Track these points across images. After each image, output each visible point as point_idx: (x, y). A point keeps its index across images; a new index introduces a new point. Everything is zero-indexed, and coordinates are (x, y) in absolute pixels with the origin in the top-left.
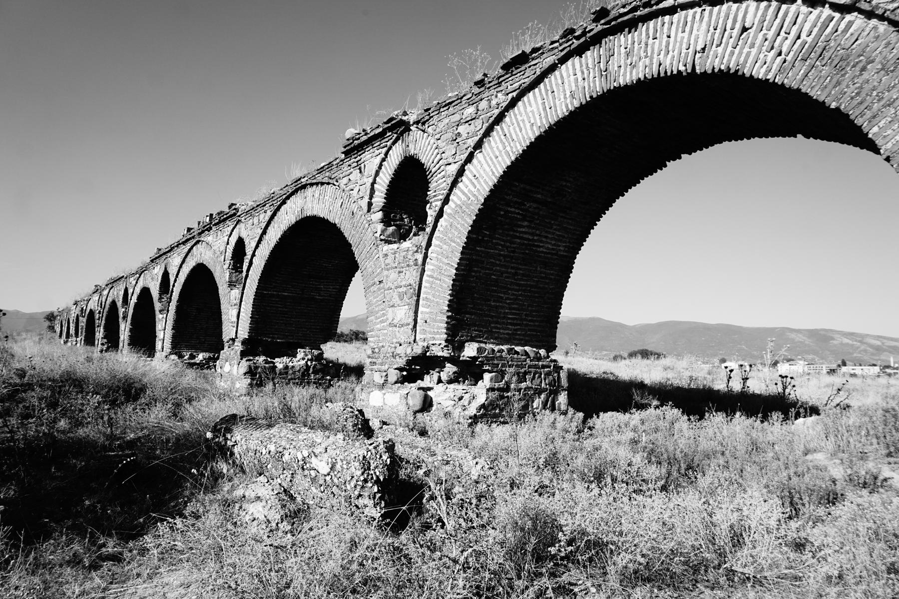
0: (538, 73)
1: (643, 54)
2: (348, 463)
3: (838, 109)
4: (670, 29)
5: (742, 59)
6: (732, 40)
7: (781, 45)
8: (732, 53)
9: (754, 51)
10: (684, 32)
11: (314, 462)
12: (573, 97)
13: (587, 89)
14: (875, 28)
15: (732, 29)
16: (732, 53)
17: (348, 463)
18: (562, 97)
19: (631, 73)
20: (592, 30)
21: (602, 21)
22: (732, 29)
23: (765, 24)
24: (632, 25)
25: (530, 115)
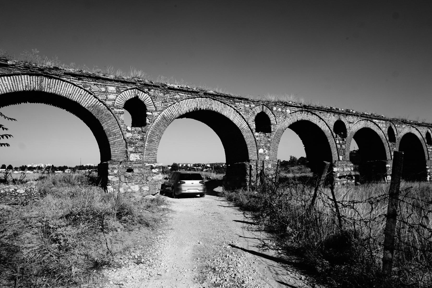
0: (12, 73)
1: (53, 87)
2: (33, 189)
3: (97, 119)
4: (62, 85)
5: (80, 101)
6: (85, 100)
7: (88, 102)
8: (78, 99)
9: (83, 101)
10: (66, 87)
11: (18, 191)
12: (26, 87)
13: (32, 87)
14: (105, 107)
15: (78, 93)
16: (78, 99)
17: (33, 189)
18: (21, 85)
19: (49, 90)
20: (38, 72)
21: (42, 72)
22: (78, 93)
23: (86, 96)
24: (51, 78)
25: (5, 84)
